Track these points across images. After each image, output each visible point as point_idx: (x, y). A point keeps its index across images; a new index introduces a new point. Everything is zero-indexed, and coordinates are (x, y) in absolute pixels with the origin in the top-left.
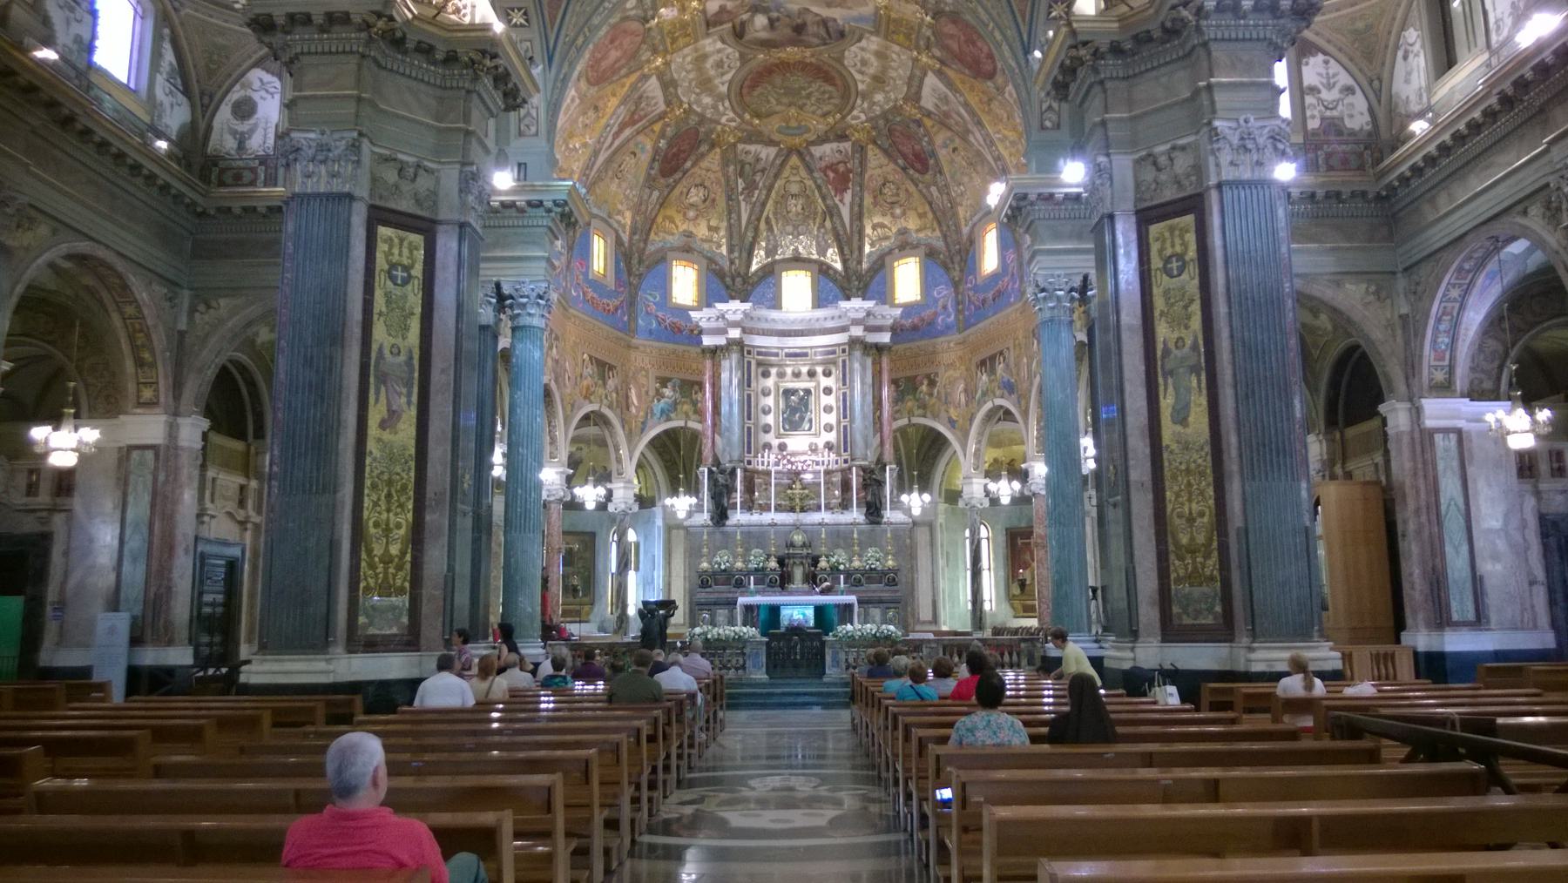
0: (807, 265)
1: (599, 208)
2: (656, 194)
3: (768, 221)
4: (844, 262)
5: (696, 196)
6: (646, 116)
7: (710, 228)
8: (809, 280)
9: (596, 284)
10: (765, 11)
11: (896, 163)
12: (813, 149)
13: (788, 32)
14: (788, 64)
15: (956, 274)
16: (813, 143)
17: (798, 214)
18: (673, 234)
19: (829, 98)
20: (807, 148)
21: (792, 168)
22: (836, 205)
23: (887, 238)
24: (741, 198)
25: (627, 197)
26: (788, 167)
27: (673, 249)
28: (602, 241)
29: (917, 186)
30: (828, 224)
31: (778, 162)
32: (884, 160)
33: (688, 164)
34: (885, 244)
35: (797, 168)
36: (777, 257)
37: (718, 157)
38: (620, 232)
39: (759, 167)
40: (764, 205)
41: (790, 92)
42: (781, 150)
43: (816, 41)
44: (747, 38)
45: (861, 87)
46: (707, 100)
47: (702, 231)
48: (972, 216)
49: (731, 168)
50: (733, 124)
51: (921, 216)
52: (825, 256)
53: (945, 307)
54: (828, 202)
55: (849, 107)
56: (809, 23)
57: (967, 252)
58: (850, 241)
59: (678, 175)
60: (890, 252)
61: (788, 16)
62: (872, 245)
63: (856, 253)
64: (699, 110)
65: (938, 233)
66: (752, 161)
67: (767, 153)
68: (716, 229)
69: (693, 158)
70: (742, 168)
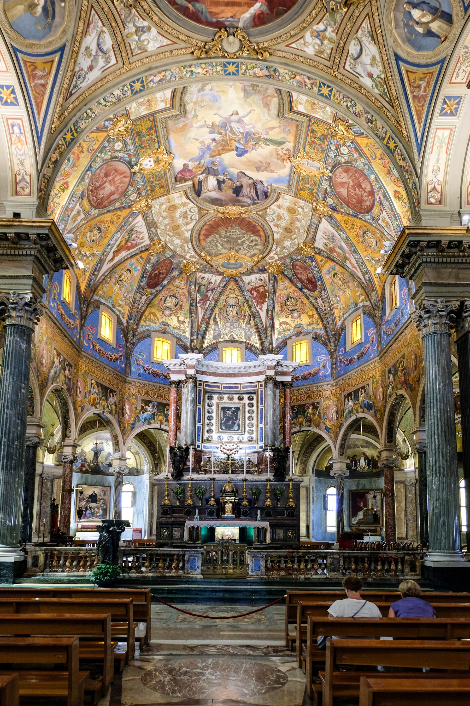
3: (215, 320)
4: (262, 343)
13: (230, 193)
15: (332, 348)
17: (233, 316)
30: (252, 322)
34: (288, 333)
36: (220, 340)
40: (212, 310)
41: (230, 241)
58: (265, 331)
60: (290, 337)
63: (269, 338)
66: (206, 283)
68: (183, 322)
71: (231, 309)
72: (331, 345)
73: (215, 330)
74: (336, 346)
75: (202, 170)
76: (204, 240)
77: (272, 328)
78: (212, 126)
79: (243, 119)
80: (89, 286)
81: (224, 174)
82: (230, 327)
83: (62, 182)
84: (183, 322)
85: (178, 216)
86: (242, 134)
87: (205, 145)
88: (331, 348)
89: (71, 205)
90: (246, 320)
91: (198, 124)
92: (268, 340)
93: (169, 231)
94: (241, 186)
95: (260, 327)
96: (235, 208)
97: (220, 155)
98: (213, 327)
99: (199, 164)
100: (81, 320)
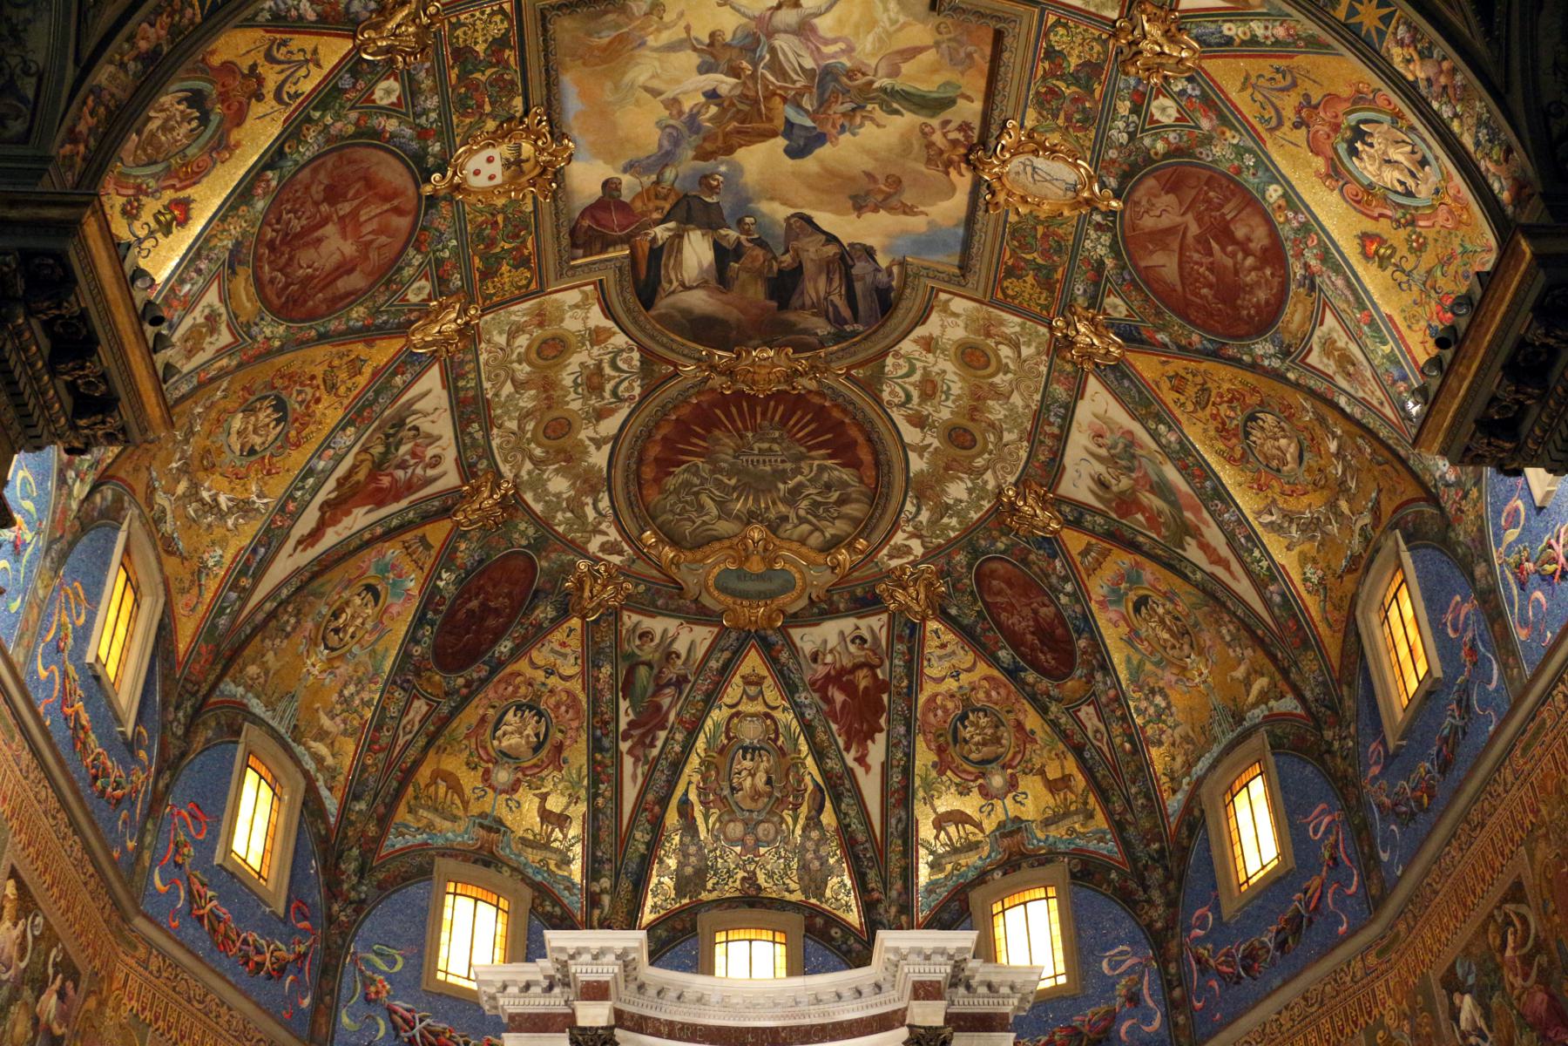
0: (773, 915)
1: (270, 705)
2: (420, 707)
3: (685, 808)
5: (516, 734)
6: (410, 487)
7: (545, 815)
8: (781, 950)
9: (232, 879)
10: (709, 220)
11: (994, 661)
12: (796, 633)
14: (752, 400)
15: (1158, 914)
16: (797, 619)
17: (756, 795)
18: (454, 819)
19: (842, 502)
20: (783, 630)
21: (747, 681)
22: (851, 772)
23: (972, 846)
24: (624, 746)
25: (346, 701)
26: (737, 679)
27: (449, 852)
28: (266, 793)
29: (1043, 710)
30: (828, 818)
31: (713, 664)
32: (966, 658)
33: (505, 647)
34: (972, 860)
35: (759, 681)
36: (704, 896)
37: (575, 643)
38: (320, 784)
39: (671, 673)
40: (677, 766)
42: (724, 631)
43: (823, 328)
44: (663, 305)
45: (917, 464)
46: (559, 485)
47: (525, 815)
48: (1189, 766)
49: (606, 670)
50: (616, 559)
51: (1053, 786)
52: (820, 895)
53: (1134, 998)
54: (830, 764)
55: (885, 525)
56: (809, 268)
57: (1185, 851)
59: (477, 672)
60: (982, 877)
61: (760, 243)
62: (935, 866)
63: (898, 885)
64: (538, 508)
65: (1100, 821)
67: (692, 639)
69: (518, 631)
70: (631, 671)
71: (747, 764)
72: (1150, 901)
73: (686, 855)
74: (1171, 904)
75: (667, 207)
76: (657, 481)
77: (905, 843)
78: (711, 45)
79: (817, 21)
80: (208, 631)
81: (740, 222)
82: (742, 842)
83: (169, 195)
84: (562, 820)
85: (568, 381)
86: (810, 74)
87: (681, 113)
88: (1155, 915)
89: (187, 287)
90: (804, 810)
91: (665, 37)
92: (894, 894)
93: (534, 439)
94: (797, 271)
95: (861, 837)
96: (772, 353)
97: (730, 150)
98: (677, 838)
99: (657, 183)
100: (159, 772)
